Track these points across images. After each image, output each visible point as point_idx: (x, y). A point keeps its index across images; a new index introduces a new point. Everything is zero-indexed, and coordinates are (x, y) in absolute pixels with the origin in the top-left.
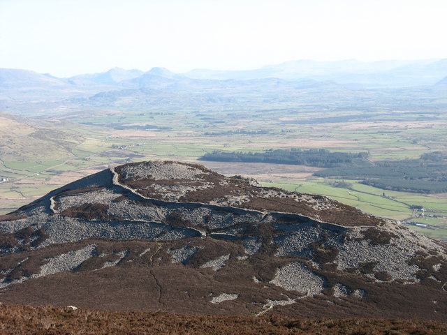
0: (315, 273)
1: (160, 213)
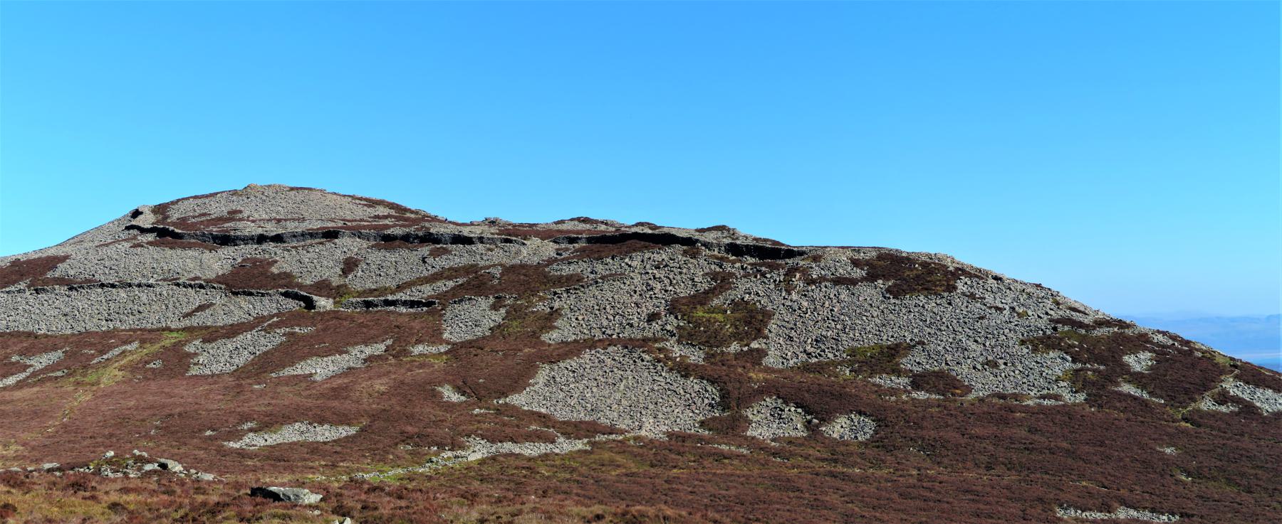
0: (685, 370)
1: (218, 262)
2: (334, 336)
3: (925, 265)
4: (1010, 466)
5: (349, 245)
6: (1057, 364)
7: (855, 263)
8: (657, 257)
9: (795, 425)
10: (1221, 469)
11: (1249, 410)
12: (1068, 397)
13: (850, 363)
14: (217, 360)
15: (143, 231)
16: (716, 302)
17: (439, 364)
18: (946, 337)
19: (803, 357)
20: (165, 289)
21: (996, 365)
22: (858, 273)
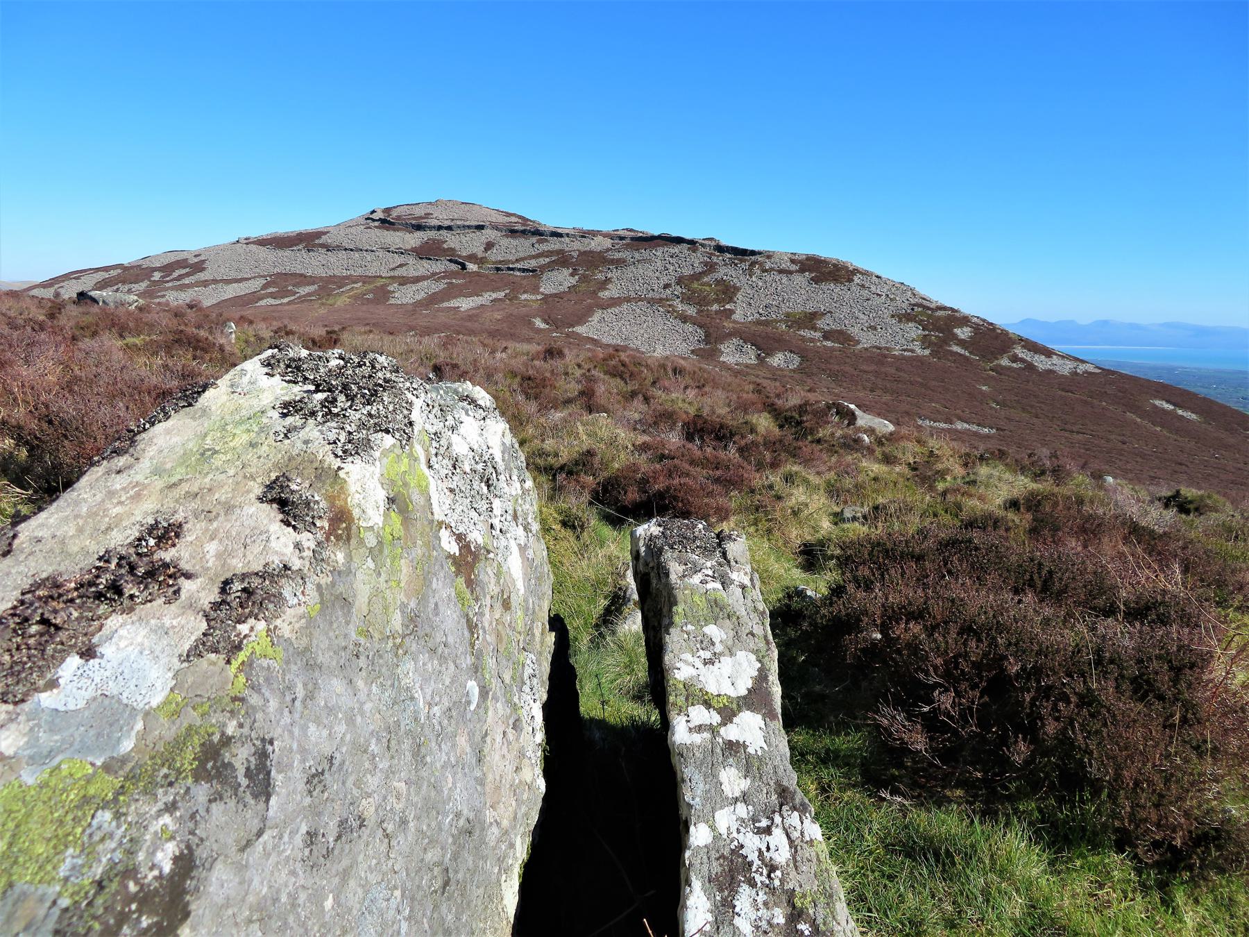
0: (684, 319)
1: (414, 240)
2: (475, 285)
3: (835, 265)
4: (885, 390)
5: (489, 234)
6: (913, 331)
7: (793, 261)
8: (672, 251)
9: (749, 356)
10: (1018, 402)
11: (1030, 367)
12: (919, 351)
13: (786, 322)
14: (406, 296)
15: (374, 220)
16: (706, 279)
17: (535, 306)
18: (846, 309)
19: (757, 316)
20: (381, 254)
21: (875, 329)
22: (794, 267)
